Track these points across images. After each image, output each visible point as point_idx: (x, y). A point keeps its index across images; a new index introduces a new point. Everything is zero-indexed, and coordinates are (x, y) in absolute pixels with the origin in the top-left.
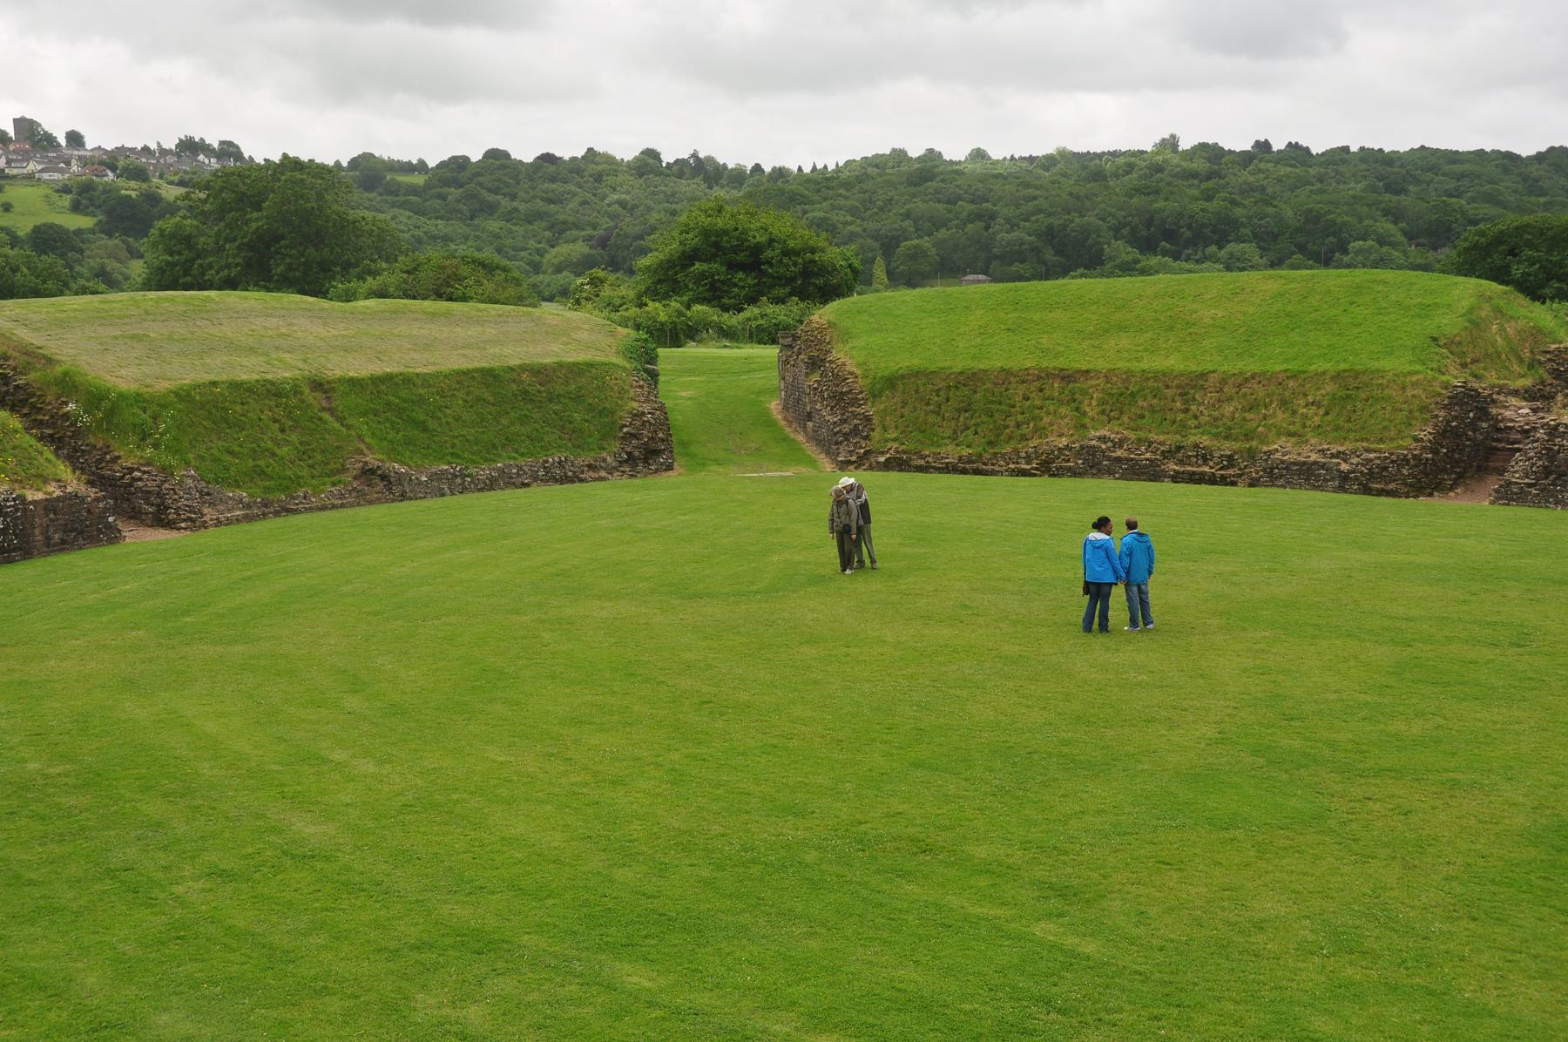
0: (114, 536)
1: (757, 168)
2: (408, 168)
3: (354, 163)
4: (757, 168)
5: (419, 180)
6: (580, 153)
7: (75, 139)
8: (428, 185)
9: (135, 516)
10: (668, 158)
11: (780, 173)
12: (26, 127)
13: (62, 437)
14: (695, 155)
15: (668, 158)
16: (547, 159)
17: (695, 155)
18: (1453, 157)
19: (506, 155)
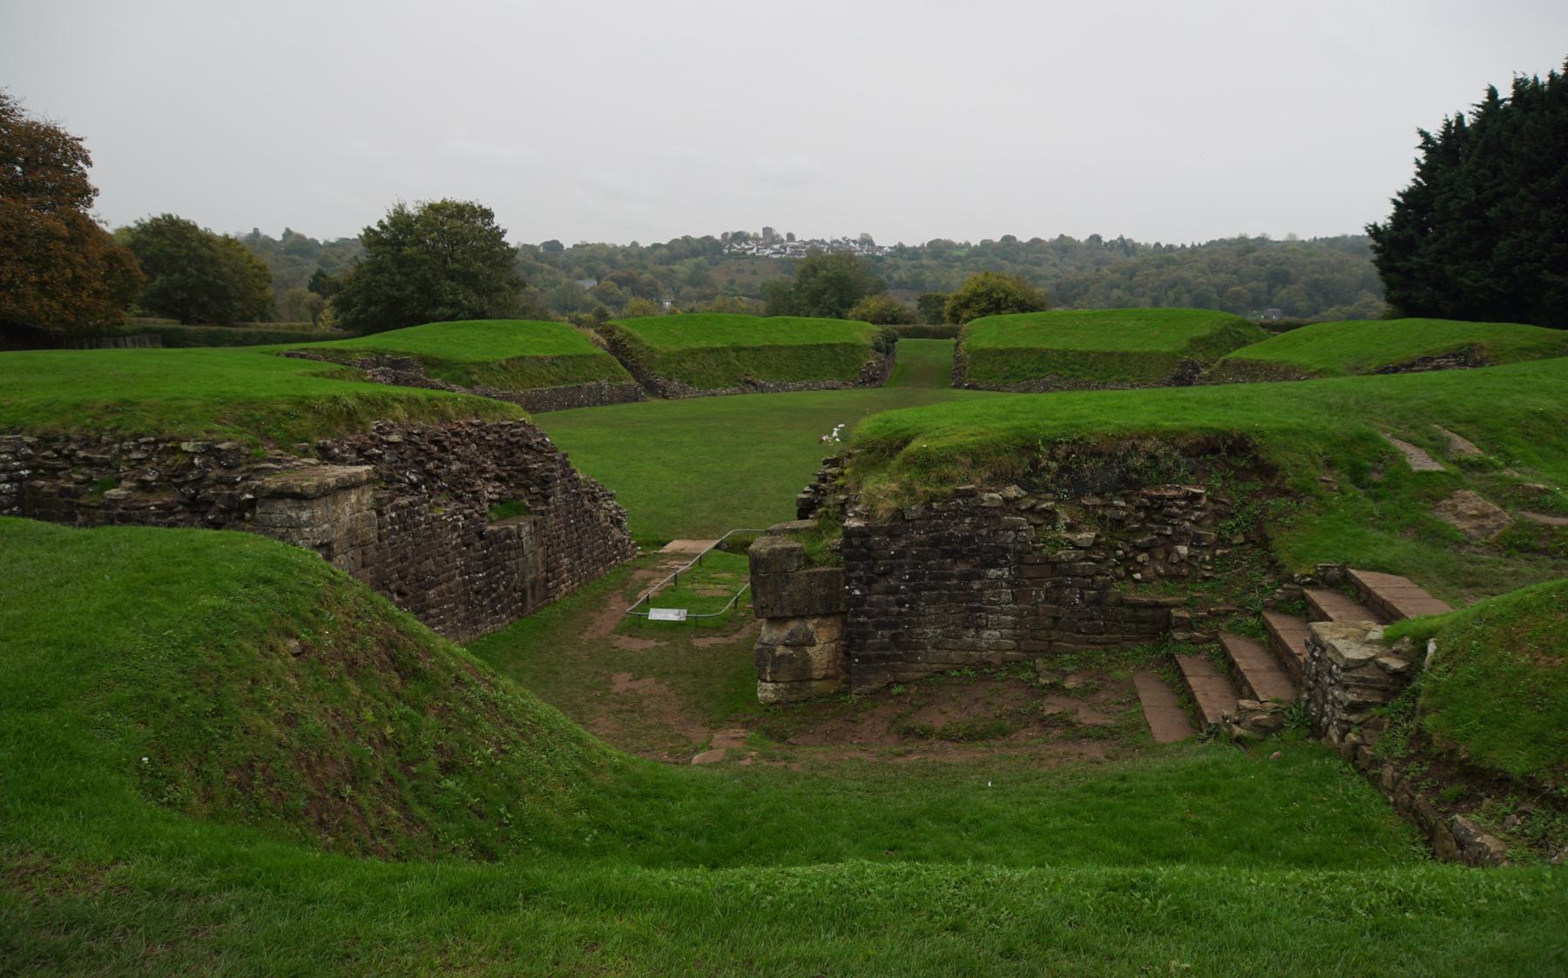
0: (644, 399)
1: (1158, 244)
2: (960, 247)
3: (931, 244)
4: (1158, 244)
5: (962, 253)
6: (1056, 237)
7: (791, 237)
8: (968, 256)
9: (656, 395)
10: (1106, 239)
11: (1170, 248)
12: (767, 231)
13: (635, 370)
14: (1121, 238)
15: (1106, 239)
16: (1036, 241)
17: (1121, 238)
18: (1166, 256)
19: (1014, 238)
